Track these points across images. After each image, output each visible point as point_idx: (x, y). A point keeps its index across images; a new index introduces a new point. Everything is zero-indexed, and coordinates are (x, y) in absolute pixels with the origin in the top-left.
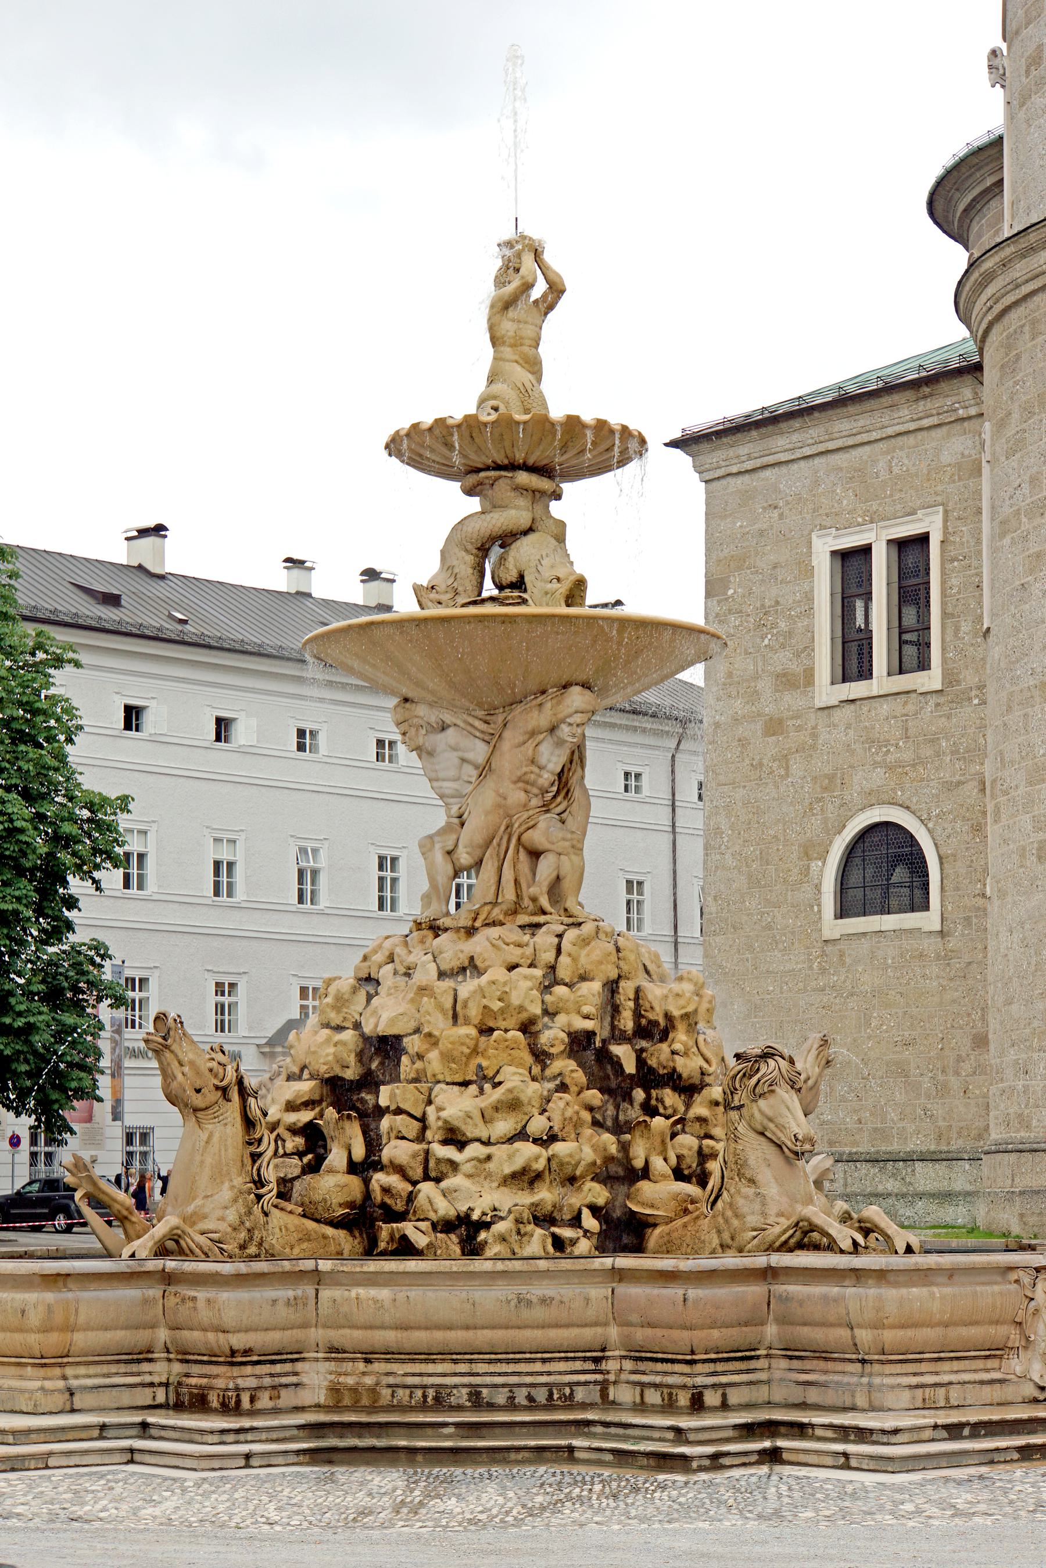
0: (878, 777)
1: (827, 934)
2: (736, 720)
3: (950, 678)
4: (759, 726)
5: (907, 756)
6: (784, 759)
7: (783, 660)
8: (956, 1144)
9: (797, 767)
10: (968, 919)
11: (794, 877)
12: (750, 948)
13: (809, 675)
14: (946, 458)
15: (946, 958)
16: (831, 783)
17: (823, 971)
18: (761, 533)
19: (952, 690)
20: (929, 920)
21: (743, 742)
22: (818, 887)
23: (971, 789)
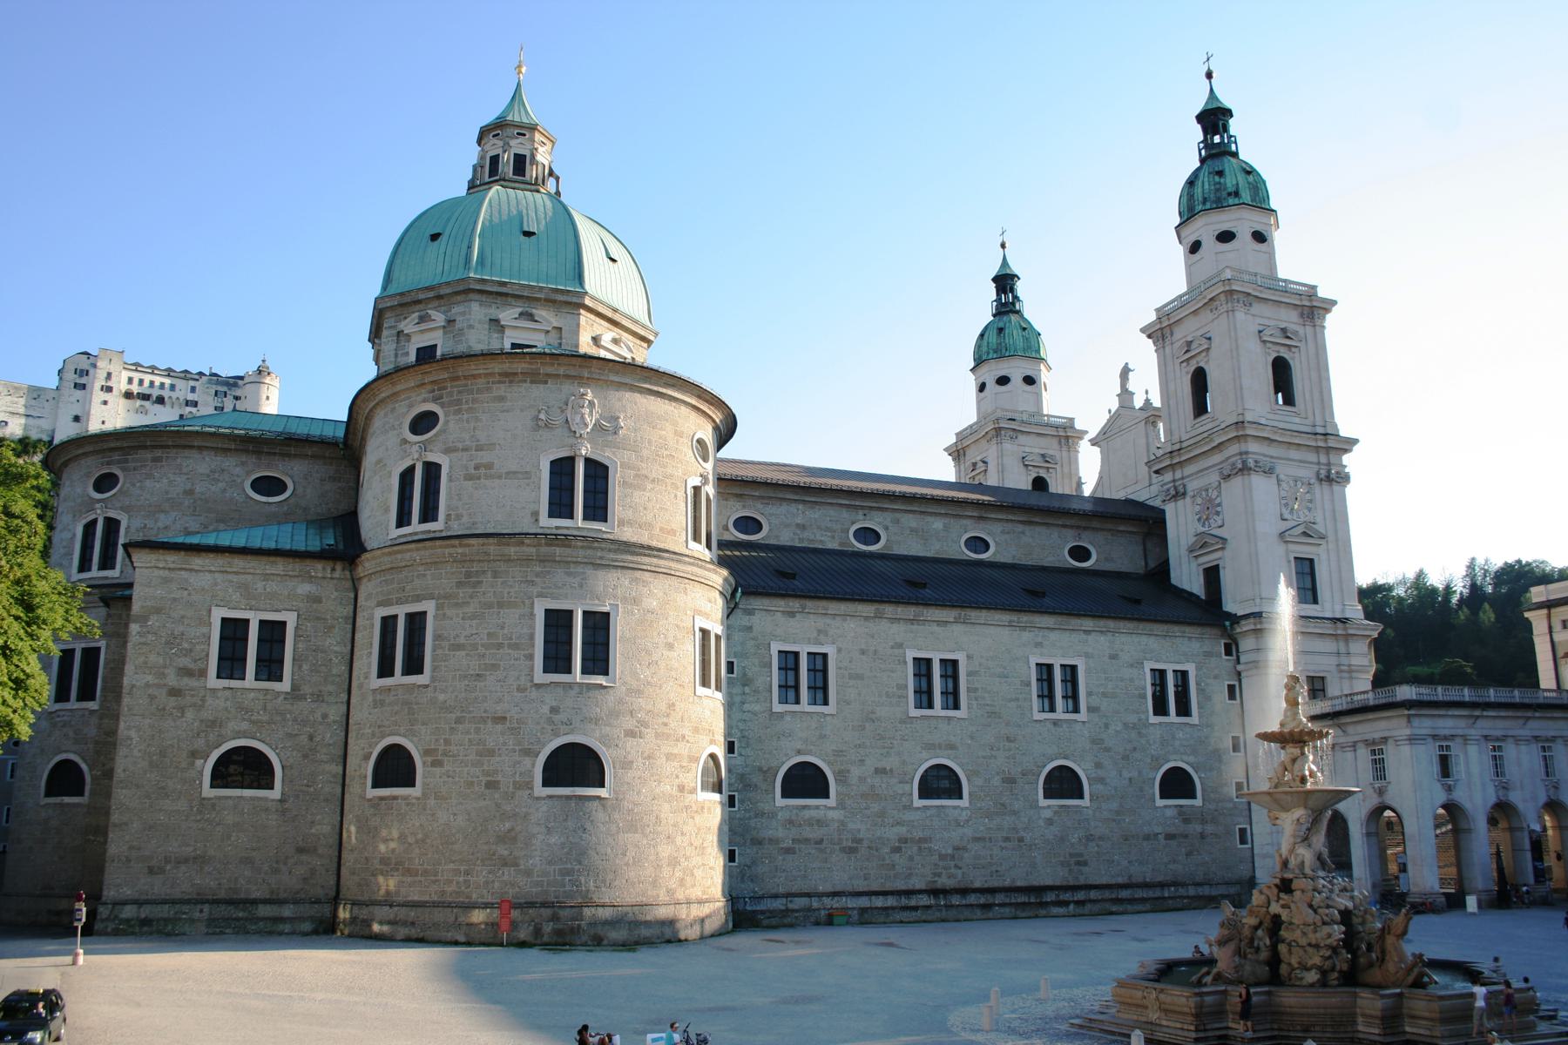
0: (245, 726)
1: (204, 794)
2: (147, 685)
3: (295, 687)
4: (164, 691)
5: (265, 718)
6: (182, 710)
7: (185, 662)
8: (283, 895)
9: (190, 714)
10: (297, 797)
11: (184, 765)
12: (148, 797)
13: (203, 673)
14: (299, 591)
15: (284, 812)
16: (213, 724)
17: (199, 812)
18: (175, 599)
19: (296, 693)
20: (275, 794)
21: (152, 697)
22: (201, 773)
23: (304, 739)
